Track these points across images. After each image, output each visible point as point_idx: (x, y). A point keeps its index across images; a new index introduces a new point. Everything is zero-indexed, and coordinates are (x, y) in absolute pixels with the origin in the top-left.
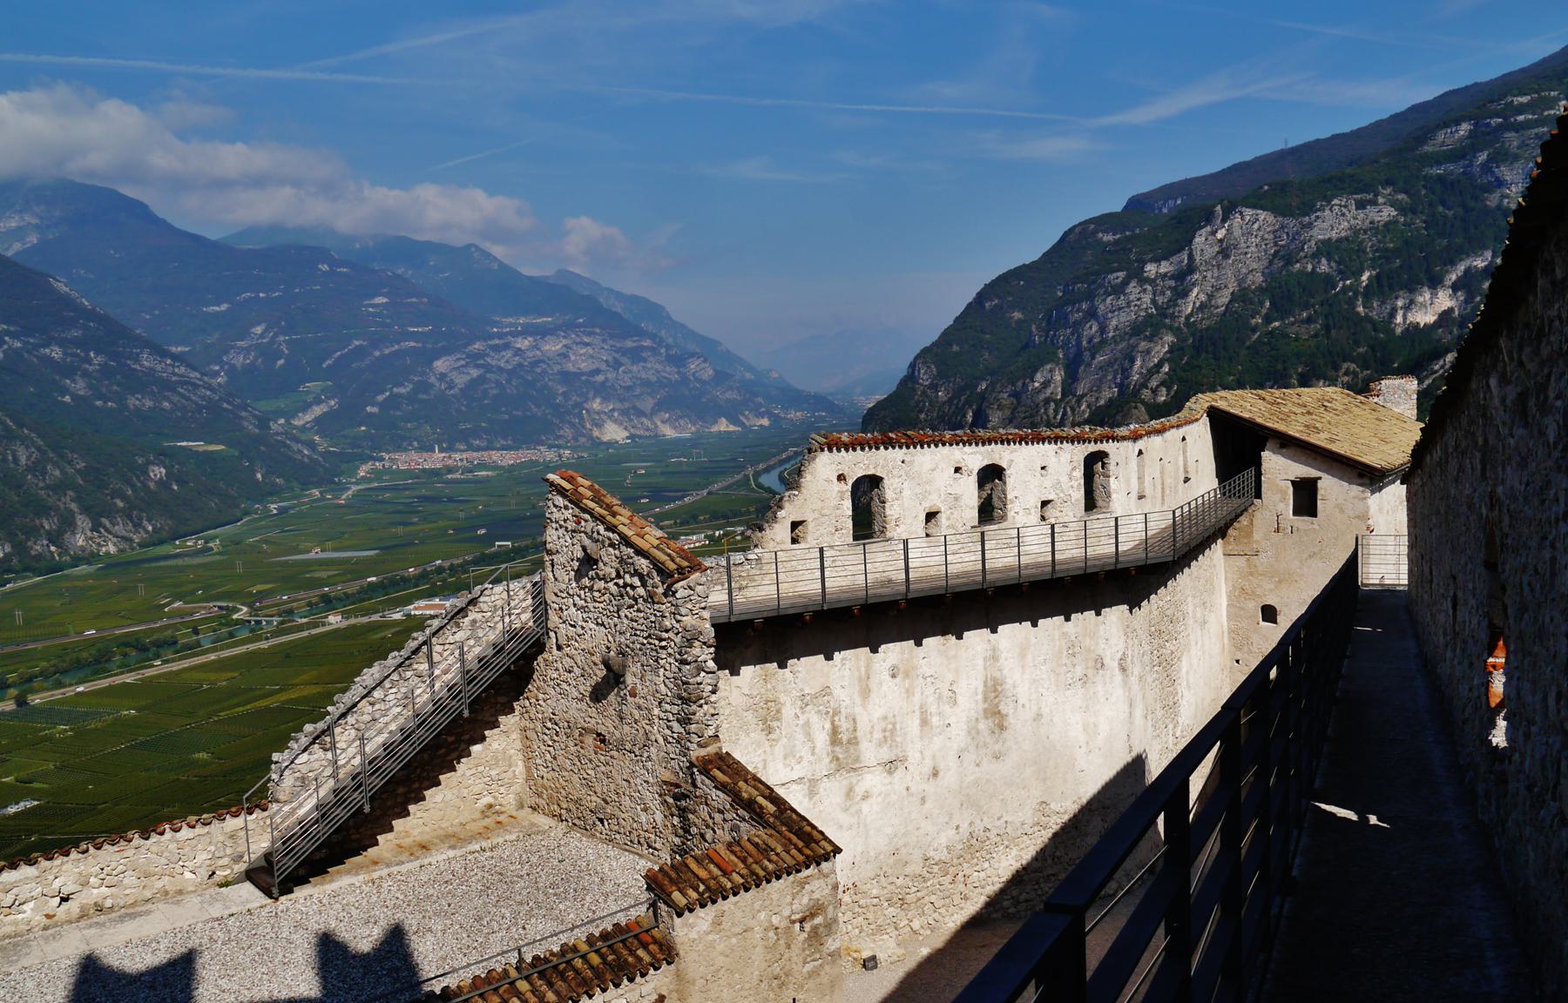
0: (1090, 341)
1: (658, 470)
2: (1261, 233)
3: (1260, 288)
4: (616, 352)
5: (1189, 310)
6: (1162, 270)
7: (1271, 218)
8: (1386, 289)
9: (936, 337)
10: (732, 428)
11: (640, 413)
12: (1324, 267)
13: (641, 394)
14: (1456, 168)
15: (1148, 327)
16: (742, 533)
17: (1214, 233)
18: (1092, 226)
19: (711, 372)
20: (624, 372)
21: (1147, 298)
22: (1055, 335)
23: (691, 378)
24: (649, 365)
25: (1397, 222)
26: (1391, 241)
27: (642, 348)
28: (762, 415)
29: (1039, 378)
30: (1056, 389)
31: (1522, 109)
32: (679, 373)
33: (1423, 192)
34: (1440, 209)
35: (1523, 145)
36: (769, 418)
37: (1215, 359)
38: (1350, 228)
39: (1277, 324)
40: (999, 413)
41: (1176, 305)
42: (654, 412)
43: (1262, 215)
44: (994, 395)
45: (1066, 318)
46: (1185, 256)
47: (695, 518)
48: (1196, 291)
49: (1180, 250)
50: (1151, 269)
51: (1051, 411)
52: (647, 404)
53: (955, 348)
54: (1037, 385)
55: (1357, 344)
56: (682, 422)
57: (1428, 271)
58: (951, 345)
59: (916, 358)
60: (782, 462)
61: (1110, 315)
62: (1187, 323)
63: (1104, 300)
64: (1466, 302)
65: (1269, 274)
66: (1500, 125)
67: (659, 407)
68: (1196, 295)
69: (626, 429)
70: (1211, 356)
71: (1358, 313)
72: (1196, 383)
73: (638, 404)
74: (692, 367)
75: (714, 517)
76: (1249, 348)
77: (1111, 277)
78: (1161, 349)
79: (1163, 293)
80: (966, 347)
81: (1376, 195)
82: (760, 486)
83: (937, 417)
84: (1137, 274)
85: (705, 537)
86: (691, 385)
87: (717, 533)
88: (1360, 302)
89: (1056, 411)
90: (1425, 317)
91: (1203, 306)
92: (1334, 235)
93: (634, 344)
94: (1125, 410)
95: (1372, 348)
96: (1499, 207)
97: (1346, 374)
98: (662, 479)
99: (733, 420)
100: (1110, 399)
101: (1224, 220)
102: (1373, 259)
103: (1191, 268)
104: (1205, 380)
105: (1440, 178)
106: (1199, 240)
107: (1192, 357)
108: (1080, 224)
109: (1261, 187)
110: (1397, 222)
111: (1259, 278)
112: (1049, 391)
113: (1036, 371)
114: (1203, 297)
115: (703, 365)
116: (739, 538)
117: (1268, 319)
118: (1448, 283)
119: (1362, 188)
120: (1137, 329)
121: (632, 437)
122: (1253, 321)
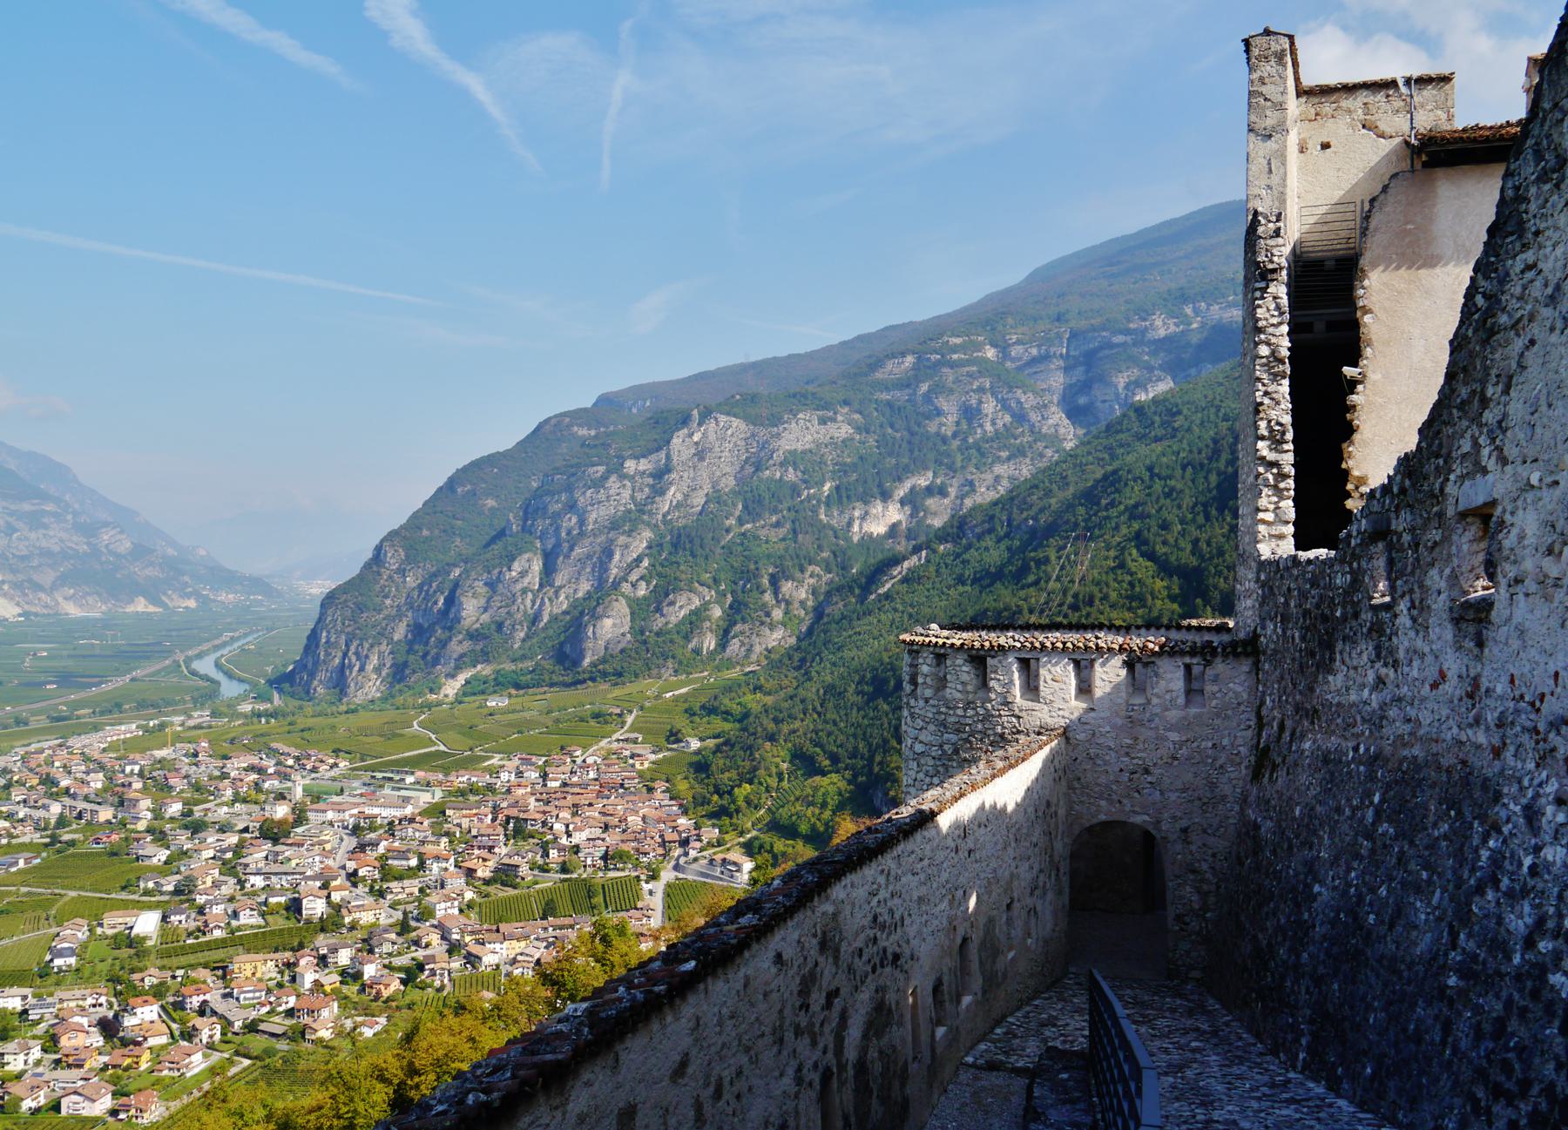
0: (569, 533)
1: (65, 653)
2: (734, 440)
3: (733, 491)
4: (12, 514)
5: (666, 508)
6: (641, 468)
7: (743, 426)
8: (845, 499)
9: (404, 520)
10: (151, 609)
11: (38, 587)
12: (791, 475)
13: (40, 566)
14: (901, 396)
15: (626, 522)
16: (182, 725)
17: (691, 435)
18: (568, 420)
19: (128, 545)
20: (19, 539)
21: (626, 494)
22: (533, 524)
23: (105, 550)
24: (51, 533)
25: (853, 439)
26: (849, 456)
27: (44, 513)
28: (188, 596)
29: (517, 566)
30: (534, 579)
31: (955, 349)
32: (88, 544)
33: (875, 414)
34: (890, 431)
35: (957, 381)
36: (197, 600)
37: (694, 556)
38: (813, 442)
39: (749, 526)
40: (474, 602)
41: (653, 503)
42: (54, 587)
43: (736, 422)
44: (469, 582)
45: (545, 508)
46: (662, 455)
47: (118, 706)
48: (673, 489)
49: (659, 449)
50: (630, 466)
51: (528, 603)
52: (47, 577)
53: (425, 533)
54: (514, 574)
55: (820, 548)
56: (90, 600)
57: (880, 485)
58: (421, 529)
59: (382, 541)
60: (217, 648)
61: (589, 508)
62: (665, 522)
63: (584, 493)
64: (911, 516)
65: (740, 481)
66: (939, 361)
67: (63, 581)
68: (673, 494)
69: (18, 604)
70: (688, 553)
71: (821, 521)
72: (675, 579)
73: (35, 577)
74: (105, 537)
75: (142, 705)
76: (723, 548)
77: (591, 470)
78: (640, 544)
79: (641, 490)
80: (437, 532)
81: (835, 413)
82: (194, 673)
83: (406, 604)
84: (617, 469)
85: (137, 727)
86: (104, 559)
87: (151, 724)
88: (822, 510)
89: (533, 602)
90: (878, 528)
91: (679, 505)
92: (799, 447)
93: (33, 508)
94: (606, 601)
95: (834, 553)
96: (938, 434)
97: (811, 576)
98: (70, 663)
99: (154, 601)
100: (588, 592)
101: (700, 424)
102: (833, 472)
103: (668, 469)
104: (684, 576)
105: (889, 404)
106: (676, 441)
107: (670, 553)
108: (556, 416)
109: (733, 397)
110: (853, 439)
111: (731, 482)
112: (526, 581)
113: (513, 560)
114: (679, 497)
115: (118, 537)
116: (179, 729)
117: (741, 522)
118: (897, 498)
119: (825, 408)
120: (615, 525)
121: (25, 614)
122: (728, 523)
